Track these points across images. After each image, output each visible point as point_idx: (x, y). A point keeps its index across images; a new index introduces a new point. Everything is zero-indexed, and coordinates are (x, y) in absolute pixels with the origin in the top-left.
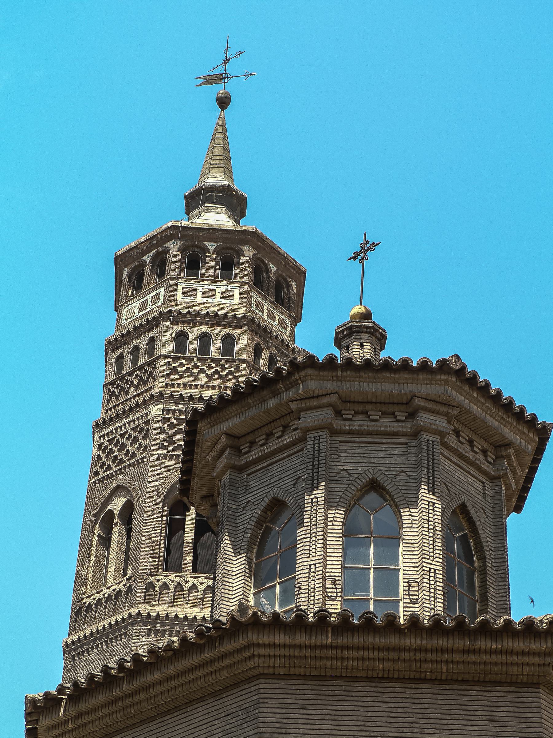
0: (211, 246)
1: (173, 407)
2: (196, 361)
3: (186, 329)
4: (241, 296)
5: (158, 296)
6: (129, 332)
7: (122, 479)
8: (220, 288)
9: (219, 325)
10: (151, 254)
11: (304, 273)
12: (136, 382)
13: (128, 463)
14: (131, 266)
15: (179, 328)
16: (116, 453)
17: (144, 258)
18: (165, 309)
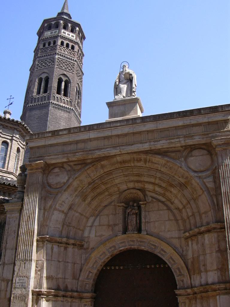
0: (70, 25)
1: (61, 57)
2: (65, 48)
3: (64, 41)
4: (76, 38)
5: (56, 31)
6: (48, 38)
7: (45, 71)
8: (71, 34)
9: (71, 42)
10: (56, 21)
11: (85, 38)
12: (50, 49)
13: (47, 67)
14: (48, 23)
15: (62, 40)
16: (44, 64)
17: (52, 22)
18: (60, 35)
